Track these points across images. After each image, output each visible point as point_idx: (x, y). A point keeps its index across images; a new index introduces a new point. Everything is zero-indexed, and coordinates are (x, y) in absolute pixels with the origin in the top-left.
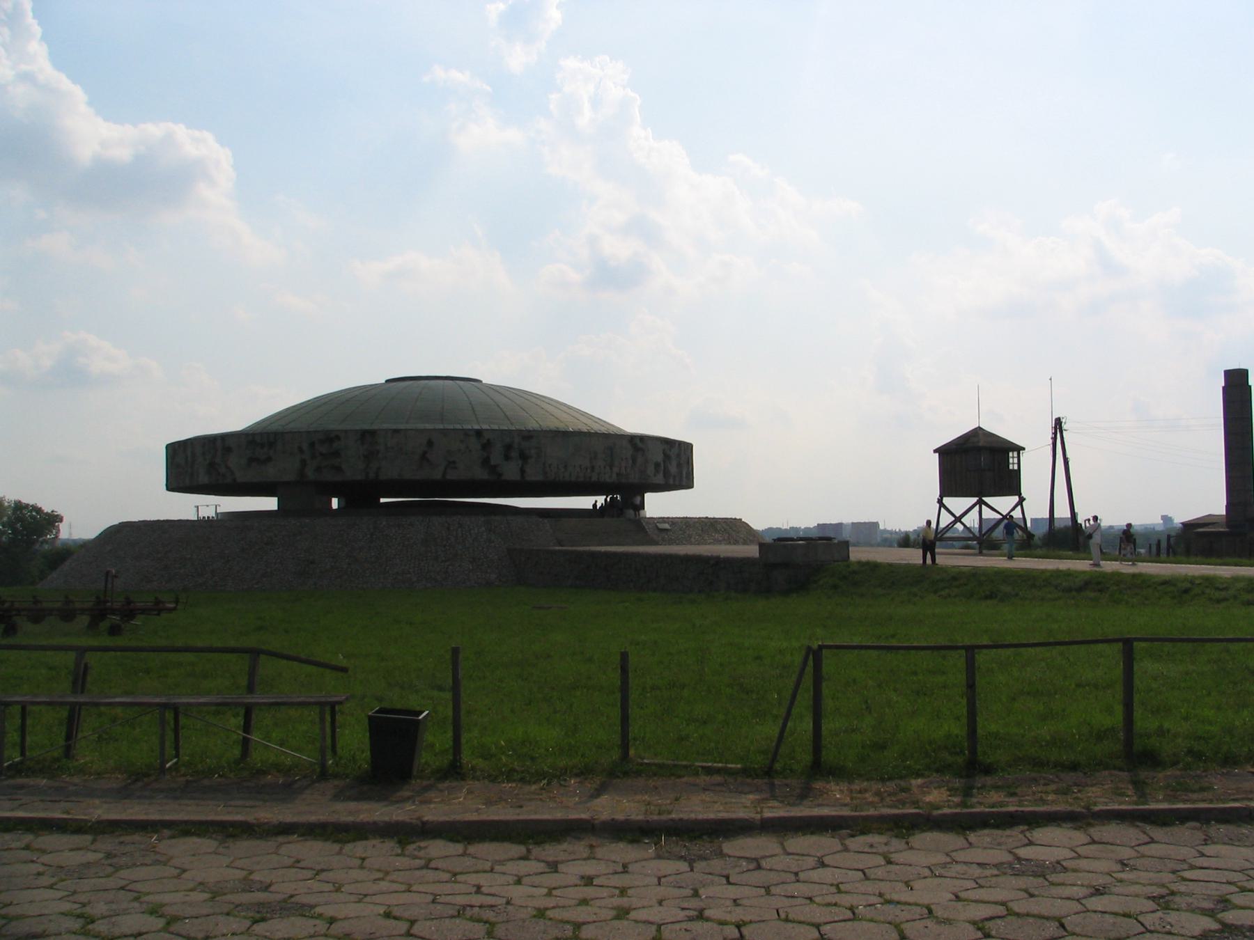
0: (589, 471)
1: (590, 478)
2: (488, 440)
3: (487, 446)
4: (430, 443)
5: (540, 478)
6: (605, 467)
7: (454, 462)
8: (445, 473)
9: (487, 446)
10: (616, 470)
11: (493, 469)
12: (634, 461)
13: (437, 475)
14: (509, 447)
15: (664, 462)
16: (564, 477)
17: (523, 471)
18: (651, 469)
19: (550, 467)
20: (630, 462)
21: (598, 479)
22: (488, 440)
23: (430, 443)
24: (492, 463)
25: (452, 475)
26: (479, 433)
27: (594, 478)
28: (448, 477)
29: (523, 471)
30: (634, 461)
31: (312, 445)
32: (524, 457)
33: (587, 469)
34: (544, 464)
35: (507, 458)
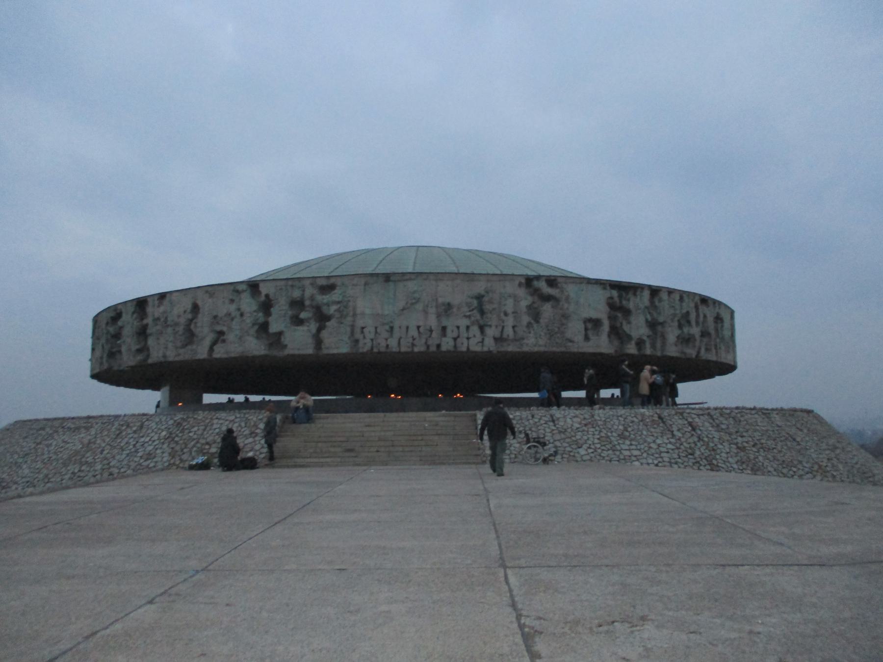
0: (434, 335)
1: (439, 346)
2: (267, 296)
3: (267, 306)
4: (195, 308)
5: (344, 349)
6: (468, 328)
7: (221, 333)
8: (211, 349)
9: (267, 306)
10: (491, 332)
11: (276, 340)
12: (536, 315)
13: (202, 352)
14: (297, 304)
15: (612, 318)
16: (387, 346)
17: (318, 342)
18: (575, 330)
19: (362, 332)
20: (526, 319)
21: (455, 346)
22: (267, 296)
23: (195, 308)
24: (274, 328)
25: (220, 352)
26: (253, 286)
27: (447, 345)
28: (216, 355)
29: (318, 342)
30: (536, 315)
31: (107, 324)
32: (322, 318)
33: (431, 331)
34: (353, 327)
35: (298, 321)
